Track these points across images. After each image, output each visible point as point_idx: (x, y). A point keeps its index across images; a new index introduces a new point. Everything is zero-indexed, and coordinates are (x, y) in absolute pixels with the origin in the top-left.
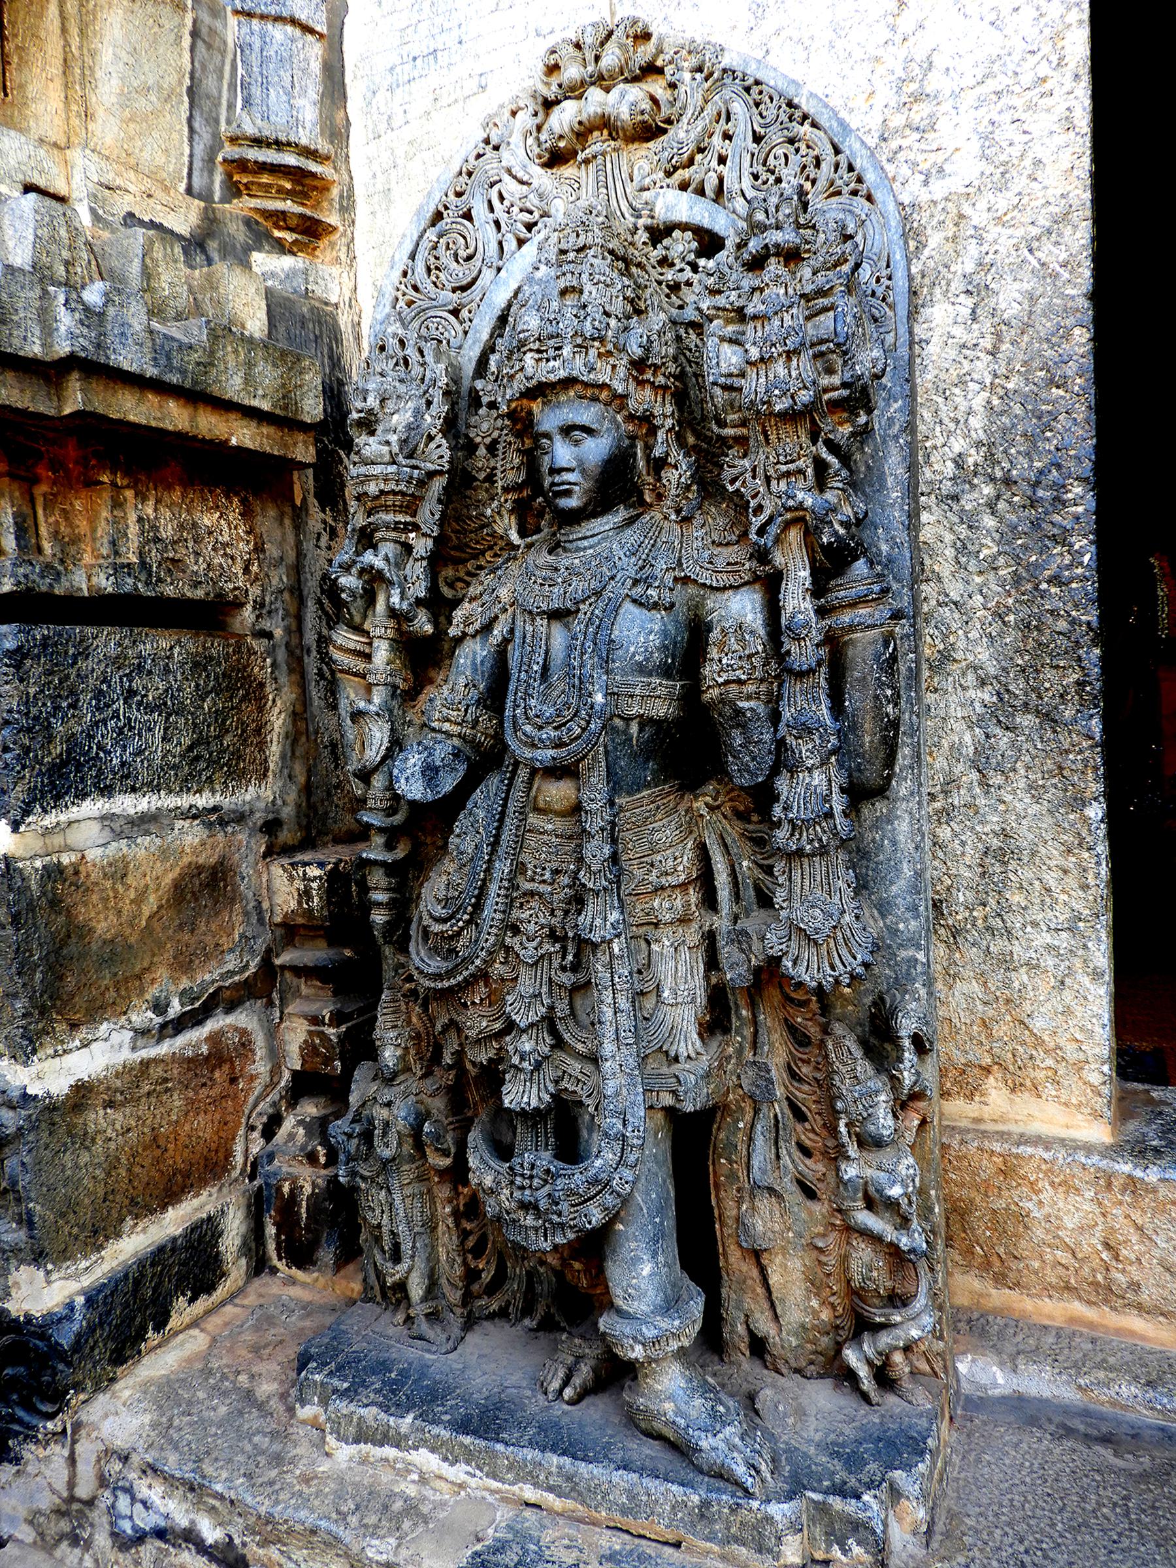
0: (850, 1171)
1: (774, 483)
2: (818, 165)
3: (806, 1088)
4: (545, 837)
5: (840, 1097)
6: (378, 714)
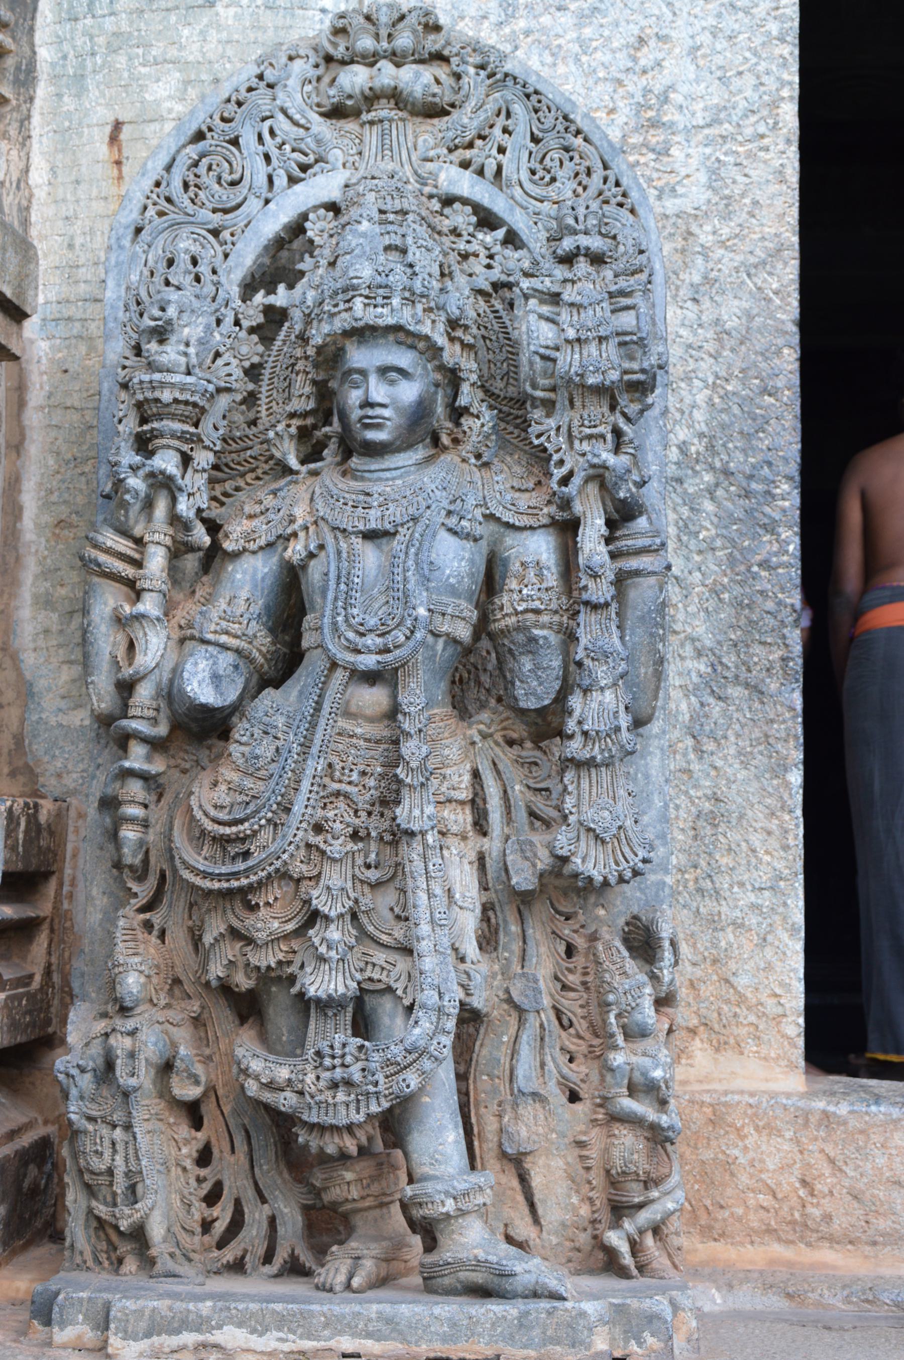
0: (618, 1059)
1: (577, 443)
2: (589, 173)
3: (572, 995)
4: (354, 740)
5: (614, 990)
6: (158, 619)
